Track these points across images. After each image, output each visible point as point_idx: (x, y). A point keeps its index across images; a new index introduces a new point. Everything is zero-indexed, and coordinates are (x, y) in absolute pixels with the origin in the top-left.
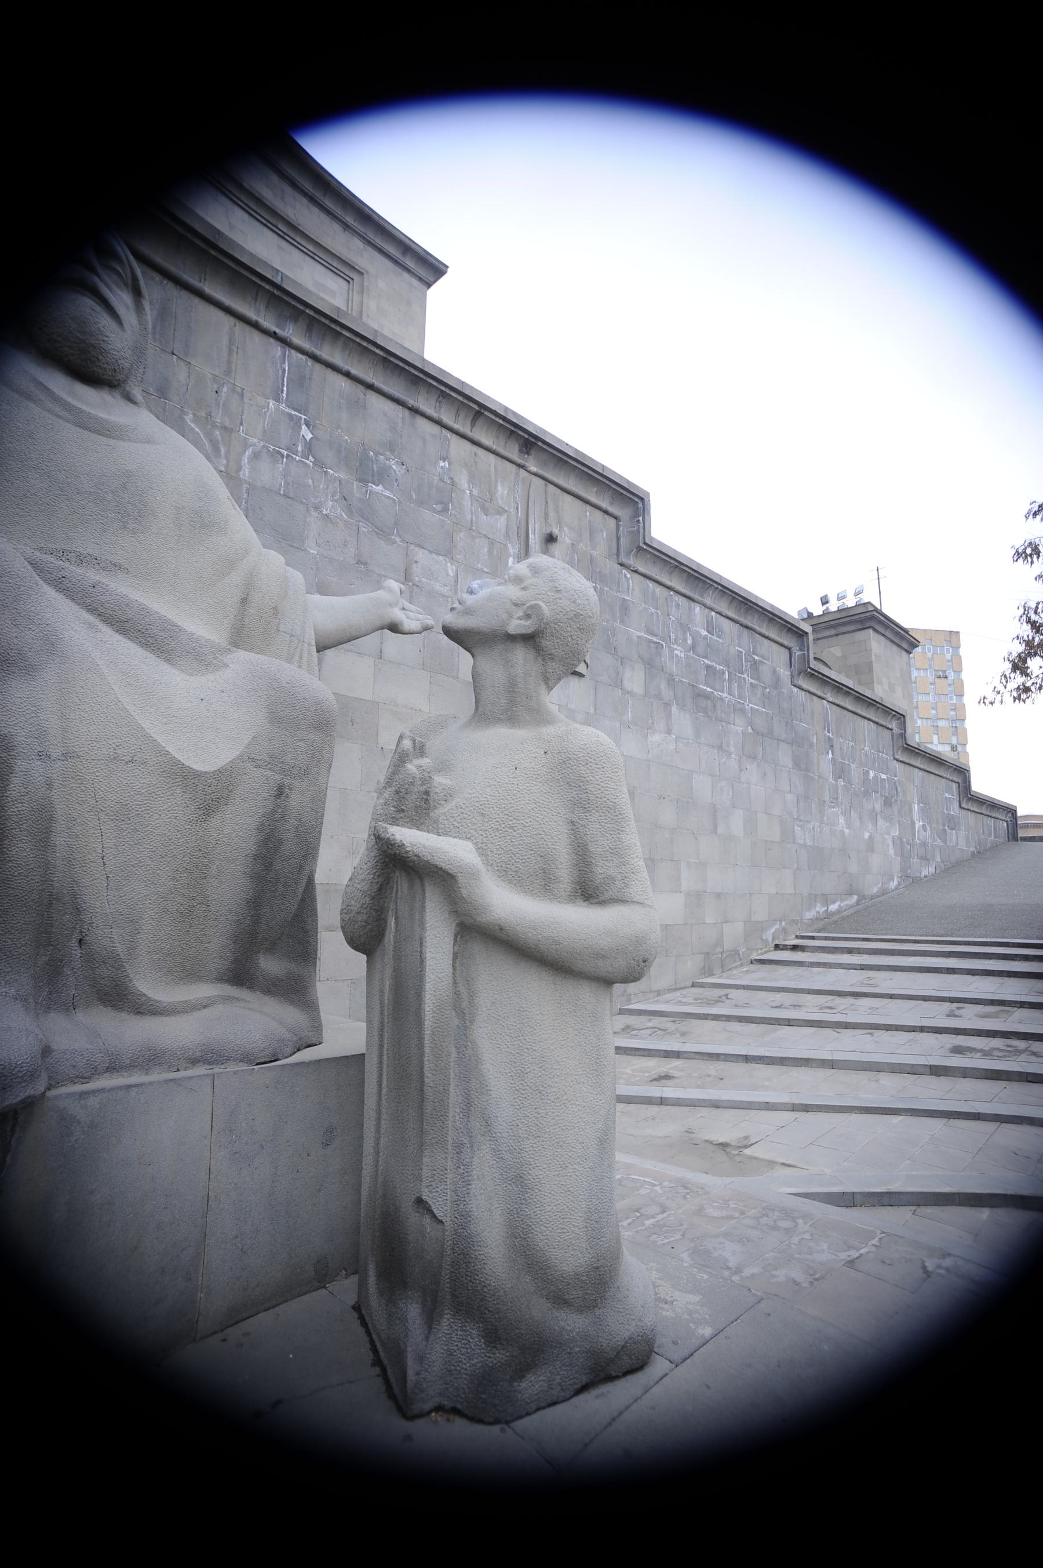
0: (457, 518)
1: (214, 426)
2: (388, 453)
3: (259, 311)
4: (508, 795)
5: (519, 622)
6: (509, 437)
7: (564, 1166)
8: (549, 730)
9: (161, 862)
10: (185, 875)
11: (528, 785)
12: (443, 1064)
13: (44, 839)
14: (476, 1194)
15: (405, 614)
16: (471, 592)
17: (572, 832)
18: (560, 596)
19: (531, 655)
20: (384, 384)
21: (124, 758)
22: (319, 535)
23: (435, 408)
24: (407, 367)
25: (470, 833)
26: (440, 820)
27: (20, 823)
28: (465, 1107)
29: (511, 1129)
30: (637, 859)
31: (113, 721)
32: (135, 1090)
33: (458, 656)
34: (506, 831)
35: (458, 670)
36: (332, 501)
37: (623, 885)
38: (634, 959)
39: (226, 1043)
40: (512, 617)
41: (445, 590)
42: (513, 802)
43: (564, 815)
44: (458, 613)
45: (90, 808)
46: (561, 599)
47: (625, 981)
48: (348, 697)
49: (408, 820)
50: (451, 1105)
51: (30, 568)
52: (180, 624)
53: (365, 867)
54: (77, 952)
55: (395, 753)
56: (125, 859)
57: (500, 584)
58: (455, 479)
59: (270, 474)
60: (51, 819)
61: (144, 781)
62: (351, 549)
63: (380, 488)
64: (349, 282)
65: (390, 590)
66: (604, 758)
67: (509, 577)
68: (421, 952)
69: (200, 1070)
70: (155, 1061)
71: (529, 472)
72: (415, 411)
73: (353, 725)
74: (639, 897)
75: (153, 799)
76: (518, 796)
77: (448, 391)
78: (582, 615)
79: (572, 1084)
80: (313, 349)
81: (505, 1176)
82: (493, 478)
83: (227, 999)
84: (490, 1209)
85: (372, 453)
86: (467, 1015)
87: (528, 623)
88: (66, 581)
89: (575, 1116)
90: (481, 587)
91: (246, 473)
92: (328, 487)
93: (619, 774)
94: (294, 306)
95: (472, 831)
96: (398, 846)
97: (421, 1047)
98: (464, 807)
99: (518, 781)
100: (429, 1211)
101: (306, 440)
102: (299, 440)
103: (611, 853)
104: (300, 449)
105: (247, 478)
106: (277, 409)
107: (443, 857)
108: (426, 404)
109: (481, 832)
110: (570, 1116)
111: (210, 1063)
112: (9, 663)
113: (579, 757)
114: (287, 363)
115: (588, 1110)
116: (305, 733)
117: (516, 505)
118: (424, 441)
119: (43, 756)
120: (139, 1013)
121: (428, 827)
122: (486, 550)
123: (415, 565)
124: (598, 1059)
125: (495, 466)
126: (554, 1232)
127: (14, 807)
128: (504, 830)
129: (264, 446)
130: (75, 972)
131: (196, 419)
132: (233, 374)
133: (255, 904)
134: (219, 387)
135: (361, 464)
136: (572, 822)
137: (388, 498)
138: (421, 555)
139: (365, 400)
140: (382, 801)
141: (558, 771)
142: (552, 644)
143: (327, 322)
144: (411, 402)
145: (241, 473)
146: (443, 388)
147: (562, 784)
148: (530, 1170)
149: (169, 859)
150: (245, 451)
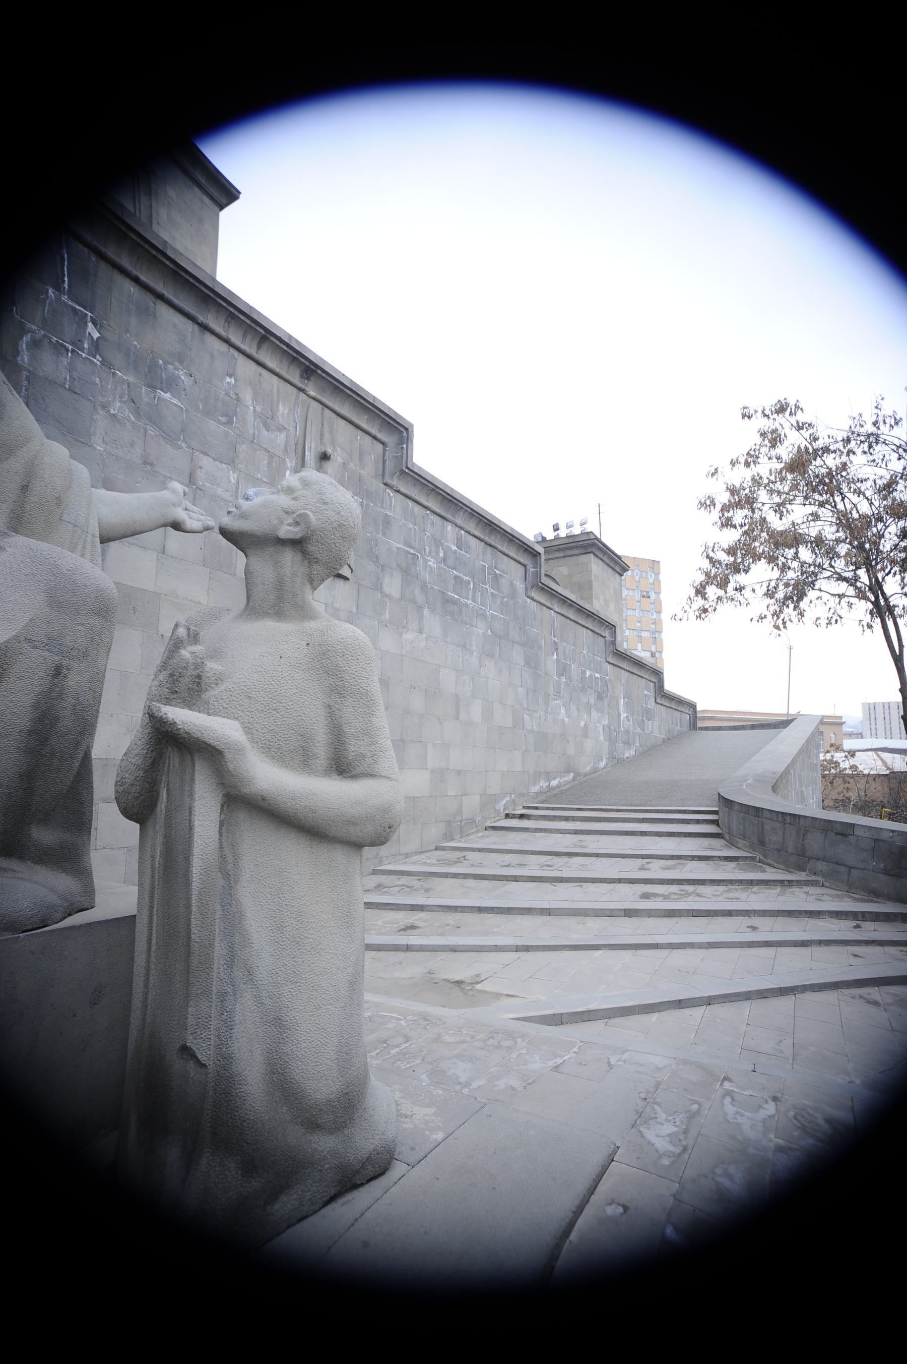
0: (240, 431)
2: (177, 363)
4: (274, 681)
5: (289, 528)
6: (292, 362)
7: (318, 1007)
8: (313, 625)
11: (291, 672)
12: (209, 921)
14: (238, 1037)
15: (188, 514)
16: (247, 499)
17: (329, 715)
18: (326, 507)
19: (298, 557)
23: (224, 327)
25: (238, 713)
26: (211, 702)
28: (229, 959)
29: (271, 977)
30: (385, 739)
33: (237, 556)
34: (270, 713)
35: (236, 568)
36: (120, 402)
37: (373, 761)
38: (381, 826)
40: (283, 524)
41: (227, 496)
42: (277, 687)
43: (322, 699)
44: (235, 516)
47: (373, 844)
48: (131, 587)
49: (181, 701)
50: (215, 958)
53: (139, 742)
55: (170, 640)
57: (273, 493)
58: (240, 395)
63: (167, 396)
65: (174, 491)
67: (282, 487)
68: (190, 820)
71: (308, 396)
72: (205, 327)
74: (386, 772)
77: (236, 313)
81: (265, 1020)
82: (275, 397)
84: (250, 1050)
85: (161, 361)
86: (232, 876)
87: (297, 529)
89: (329, 963)
90: (256, 495)
92: (116, 388)
93: (371, 665)
95: (240, 712)
96: (170, 724)
97: (188, 906)
99: (283, 668)
100: (194, 1056)
103: (362, 734)
110: (324, 963)
113: (337, 650)
115: (340, 957)
118: (212, 356)
122: (265, 462)
123: (199, 470)
124: (349, 912)
126: (309, 1066)
135: (150, 371)
136: (329, 706)
137: (176, 405)
138: (206, 462)
140: (157, 683)
141: (318, 661)
144: (201, 318)
146: (232, 310)
147: (321, 672)
148: (288, 1012)
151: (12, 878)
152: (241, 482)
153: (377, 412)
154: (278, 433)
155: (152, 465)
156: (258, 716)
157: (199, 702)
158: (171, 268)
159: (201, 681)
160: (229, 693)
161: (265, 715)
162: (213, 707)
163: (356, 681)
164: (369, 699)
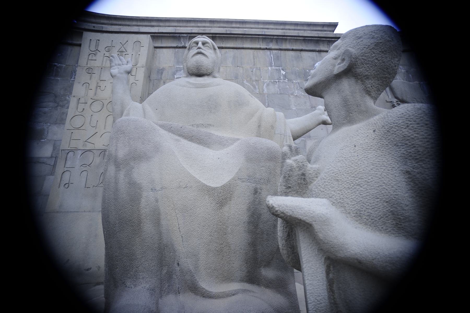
1: (253, 81)
3: (260, 44)
4: (352, 164)
10: (216, 233)
11: (365, 154)
13: (157, 222)
20: (306, 47)
21: (183, 186)
24: (313, 39)
25: (331, 194)
26: (313, 189)
31: (178, 172)
34: (355, 188)
36: (297, 90)
42: (356, 168)
43: (399, 168)
45: (172, 208)
49: (295, 192)
56: (188, 229)
59: (274, 89)
60: (159, 214)
61: (192, 194)
62: (308, 104)
65: (319, 109)
77: (330, 39)
80: (279, 47)
83: (244, 291)
85: (308, 70)
91: (266, 91)
92: (294, 86)
94: (270, 38)
98: (325, 178)
104: (282, 78)
107: (300, 212)
109: (338, 192)
112: (141, 157)
114: (272, 55)
120: (204, 297)
121: (308, 194)
127: (143, 210)
128: (353, 187)
129: (270, 81)
131: (247, 81)
133: (253, 245)
134: (252, 70)
135: (305, 75)
141: (386, 139)
143: (281, 37)
146: (328, 39)
147: (391, 146)
149: (207, 227)
150: (264, 85)
151: (252, 296)
156: (346, 192)
157: (307, 192)
158: (302, 39)
159: (305, 177)
160: (323, 181)
161: (351, 191)
162: (315, 192)
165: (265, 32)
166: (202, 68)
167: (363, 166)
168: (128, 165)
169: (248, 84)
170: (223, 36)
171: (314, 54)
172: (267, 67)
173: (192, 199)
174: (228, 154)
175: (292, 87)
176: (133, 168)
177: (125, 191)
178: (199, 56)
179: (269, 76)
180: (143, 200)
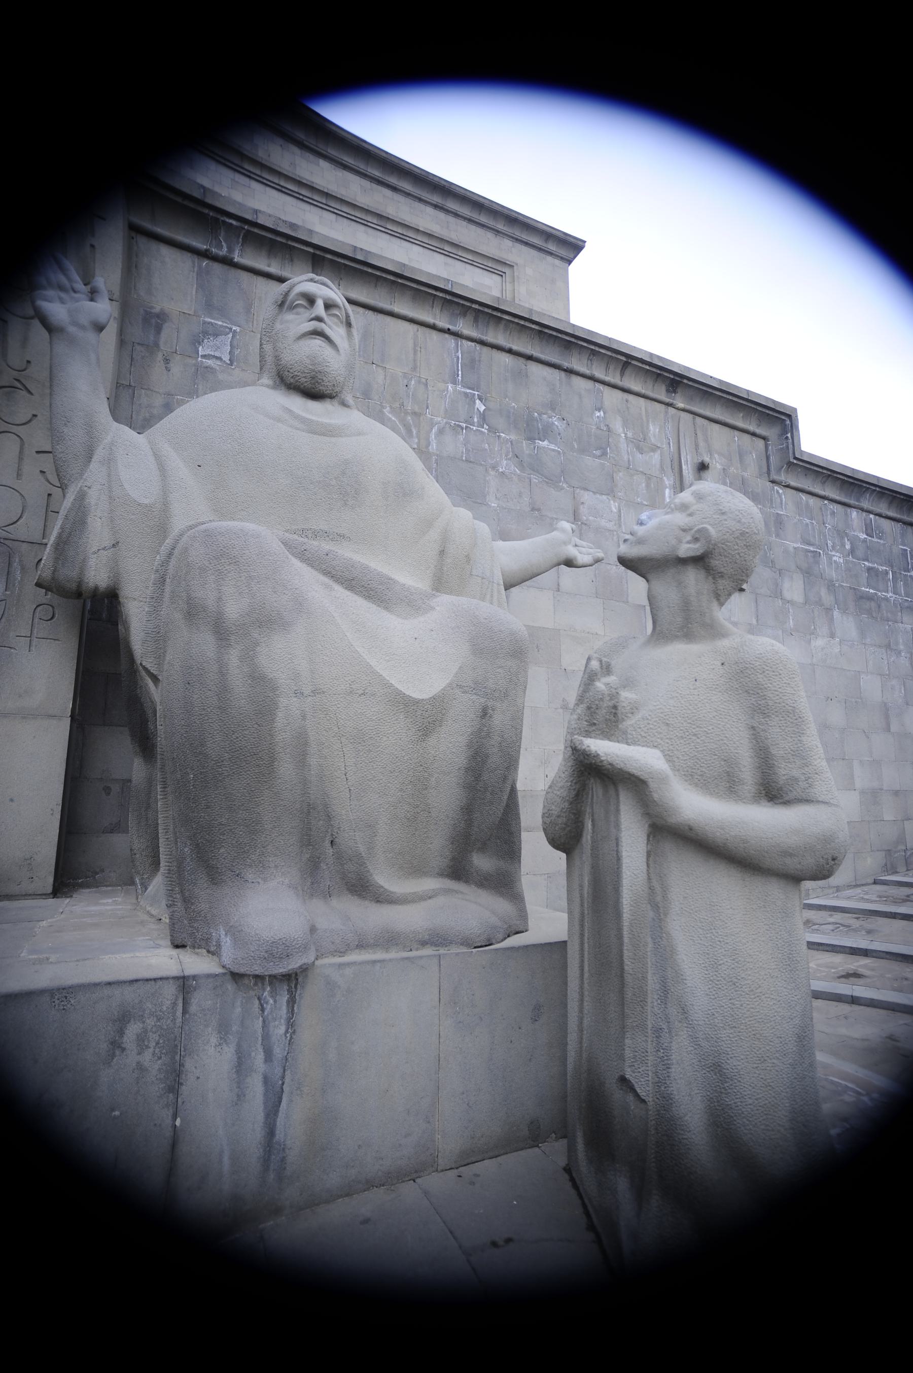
0: (615, 460)
1: (406, 413)
2: (550, 412)
3: (435, 314)
4: (691, 705)
5: (689, 546)
6: (656, 380)
7: (762, 1059)
8: (725, 643)
9: (391, 776)
11: (708, 695)
12: (641, 953)
14: (676, 1078)
15: (578, 550)
16: (641, 523)
17: (753, 737)
19: (702, 574)
20: (541, 353)
21: (358, 691)
22: (498, 490)
23: (587, 366)
24: (560, 335)
26: (629, 732)
27: (285, 748)
28: (662, 994)
29: (707, 1018)
30: (820, 760)
32: (379, 964)
33: (627, 583)
34: (690, 739)
35: (628, 596)
37: (807, 785)
38: (822, 857)
39: (448, 929)
40: (681, 542)
41: (610, 525)
42: (694, 711)
43: (745, 721)
44: (631, 543)
46: (726, 520)
47: (814, 878)
48: (533, 627)
49: (600, 732)
50: (649, 992)
51: (282, 546)
52: (393, 577)
53: (563, 775)
54: (330, 851)
55: (584, 674)
57: (667, 513)
58: (610, 426)
59: (453, 445)
61: (374, 709)
62: (526, 499)
63: (545, 443)
64: (502, 276)
65: (563, 531)
66: (780, 665)
67: (675, 506)
68: (617, 851)
69: (428, 951)
70: (393, 941)
71: (678, 409)
72: (570, 372)
73: (538, 651)
75: (381, 724)
76: (699, 705)
77: (597, 349)
78: (747, 533)
79: (765, 977)
81: (703, 1064)
83: (448, 891)
84: (690, 1095)
85: (536, 414)
86: (661, 909)
87: (697, 546)
88: (307, 553)
89: (771, 1010)
90: (650, 518)
91: (434, 447)
92: (502, 448)
93: (796, 679)
95: (659, 740)
96: (594, 756)
97: (620, 937)
98: (649, 718)
99: (699, 691)
100: (632, 1089)
101: (480, 411)
102: (474, 413)
103: (793, 755)
104: (476, 420)
105: (435, 451)
106: (455, 390)
107: (635, 765)
108: (577, 363)
109: (667, 741)
110: (765, 1009)
111: (436, 945)
113: (756, 666)
114: (460, 352)
115: (783, 1005)
116: (503, 660)
117: (668, 441)
118: (580, 397)
119: (298, 693)
120: (378, 901)
121: (618, 737)
122: (644, 485)
123: (581, 507)
125: (646, 408)
128: (688, 737)
129: (446, 423)
130: (329, 868)
131: (393, 410)
132: (418, 369)
133: (468, 810)
134: (408, 381)
135: (528, 425)
137: (554, 450)
138: (586, 497)
139: (526, 369)
140: (575, 717)
141: (736, 680)
142: (722, 563)
143: (490, 311)
144: (566, 365)
145: (430, 447)
146: (593, 347)
147: (741, 692)
148: (728, 1059)
149: (396, 774)
152: (623, 509)
153: (753, 406)
154: (652, 454)
155: (539, 510)
156: (678, 743)
157: (616, 733)
160: (646, 722)
161: (685, 741)
162: (631, 736)
163: (781, 698)
164: (797, 717)
165: (454, 285)
166: (324, 378)
167: (704, 711)
168: (248, 637)
169: (393, 418)
170: (344, 264)
171: (556, 372)
172: (445, 382)
173: (374, 718)
174: (433, 633)
175: (496, 449)
176: (257, 644)
177: (243, 693)
178: (318, 342)
179: (445, 407)
180: (280, 715)
